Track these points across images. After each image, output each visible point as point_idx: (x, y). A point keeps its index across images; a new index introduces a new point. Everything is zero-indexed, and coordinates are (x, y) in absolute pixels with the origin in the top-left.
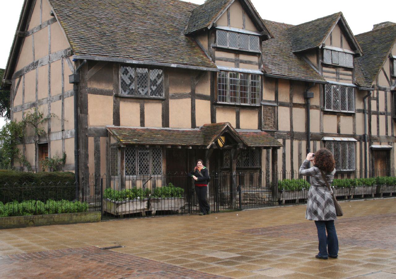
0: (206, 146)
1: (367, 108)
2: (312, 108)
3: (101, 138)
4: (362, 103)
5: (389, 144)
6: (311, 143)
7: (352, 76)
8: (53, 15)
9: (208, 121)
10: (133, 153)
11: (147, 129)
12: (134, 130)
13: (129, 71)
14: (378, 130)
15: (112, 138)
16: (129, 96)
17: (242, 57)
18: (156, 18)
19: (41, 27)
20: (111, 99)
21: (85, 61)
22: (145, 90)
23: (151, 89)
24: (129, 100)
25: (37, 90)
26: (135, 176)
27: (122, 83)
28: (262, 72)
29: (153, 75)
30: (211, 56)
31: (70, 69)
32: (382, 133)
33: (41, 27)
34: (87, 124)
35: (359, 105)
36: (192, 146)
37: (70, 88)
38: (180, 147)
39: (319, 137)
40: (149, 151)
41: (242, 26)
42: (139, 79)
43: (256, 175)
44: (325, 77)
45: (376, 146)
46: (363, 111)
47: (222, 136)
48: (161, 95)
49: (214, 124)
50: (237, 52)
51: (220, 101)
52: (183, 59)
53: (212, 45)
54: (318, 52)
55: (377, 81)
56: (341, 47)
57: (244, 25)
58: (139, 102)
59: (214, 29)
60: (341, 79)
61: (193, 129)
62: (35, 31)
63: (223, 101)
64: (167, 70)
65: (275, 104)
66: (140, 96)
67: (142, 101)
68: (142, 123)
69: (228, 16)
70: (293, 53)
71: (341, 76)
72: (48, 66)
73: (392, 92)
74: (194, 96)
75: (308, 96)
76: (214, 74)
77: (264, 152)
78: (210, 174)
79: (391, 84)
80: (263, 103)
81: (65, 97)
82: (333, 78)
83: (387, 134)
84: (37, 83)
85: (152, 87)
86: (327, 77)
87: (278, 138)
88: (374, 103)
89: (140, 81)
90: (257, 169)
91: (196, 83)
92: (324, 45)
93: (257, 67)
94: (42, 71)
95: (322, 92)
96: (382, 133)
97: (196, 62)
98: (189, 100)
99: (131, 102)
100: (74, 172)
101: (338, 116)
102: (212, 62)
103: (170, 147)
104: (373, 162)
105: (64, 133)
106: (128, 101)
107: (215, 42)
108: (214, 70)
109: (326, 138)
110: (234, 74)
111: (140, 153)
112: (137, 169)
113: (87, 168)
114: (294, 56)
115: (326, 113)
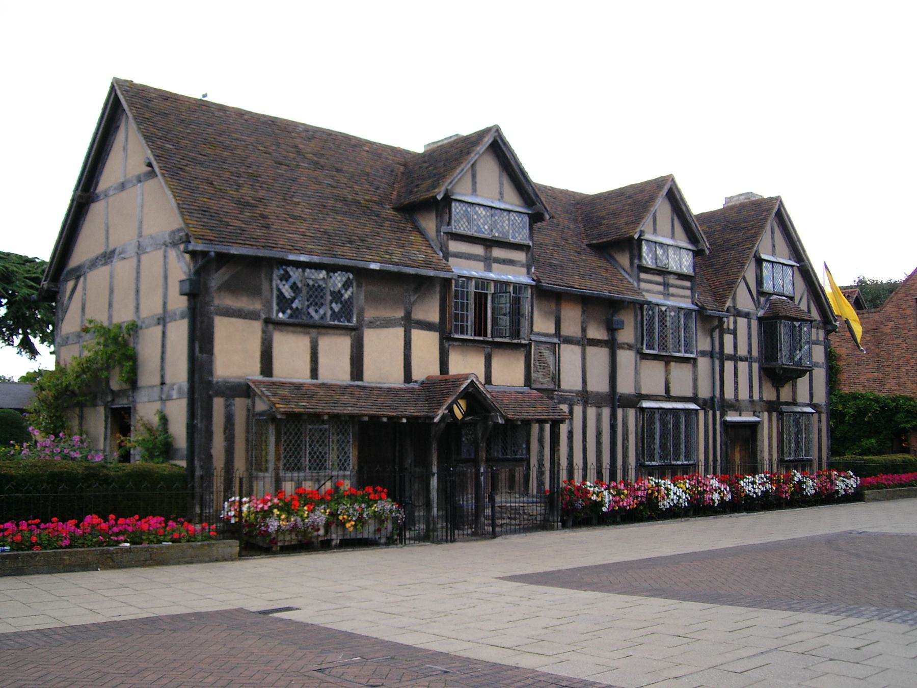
0: (434, 418)
1: (717, 349)
2: (621, 347)
3: (237, 399)
4: (709, 339)
5: (754, 415)
6: (620, 412)
7: (692, 289)
8: (150, 165)
9: (434, 370)
10: (299, 430)
11: (323, 384)
12: (298, 387)
13: (291, 273)
14: (736, 389)
15: (257, 400)
16: (292, 320)
17: (497, 253)
18: (340, 177)
19: (123, 187)
20: (257, 327)
21: (213, 254)
22: (322, 311)
23: (331, 309)
24: (291, 328)
25: (110, 305)
26: (302, 474)
27: (278, 297)
28: (533, 280)
29: (338, 280)
30: (441, 250)
31: (180, 268)
32: (744, 395)
33: (123, 187)
34: (211, 372)
35: (704, 344)
36: (407, 418)
37: (179, 303)
38: (385, 420)
39: (633, 401)
40: (327, 426)
41: (497, 196)
42: (311, 289)
43: (519, 472)
44: (644, 290)
45: (732, 417)
46: (711, 354)
47: (462, 398)
48: (349, 321)
49: (445, 377)
50: (489, 243)
51: (456, 332)
52: (391, 254)
53: (444, 228)
54: (633, 246)
55: (734, 299)
56: (673, 236)
57: (501, 194)
58: (308, 333)
59: (448, 200)
60: (673, 295)
61: (407, 385)
62: (111, 193)
63: (462, 333)
64: (362, 275)
65: (556, 340)
66: (311, 322)
67: (314, 332)
68: (314, 373)
69: (474, 176)
70: (588, 245)
71: (672, 290)
72: (135, 260)
73: (760, 319)
74: (409, 323)
75: (615, 326)
76: (446, 282)
77: (535, 428)
78: (436, 471)
79: (757, 305)
80: (533, 338)
81: (168, 320)
82: (659, 293)
83: (751, 397)
84: (111, 291)
85: (334, 305)
86: (648, 291)
87: (560, 403)
88: (728, 339)
89: (311, 293)
90: (521, 460)
91: (413, 298)
92: (642, 233)
93: (524, 270)
94: (123, 269)
95: (639, 318)
96: (744, 395)
97: (414, 261)
98: (400, 331)
99: (294, 332)
100: (183, 463)
101: (667, 364)
102: (444, 261)
103: (366, 419)
104: (727, 448)
105: (166, 388)
106: (288, 331)
107: (449, 224)
108: (447, 275)
109: (646, 404)
110: (482, 283)
111: (310, 430)
112: (306, 461)
113: (210, 457)
114: (588, 250)
115: (645, 357)
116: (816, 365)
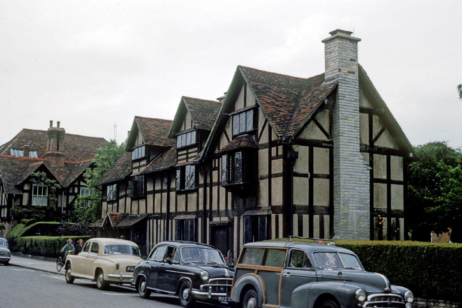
20: (106, 202)
45: (216, 220)
46: (205, 185)
74: (126, 196)
88: (215, 173)
98: (124, 199)
116: (277, 175)
